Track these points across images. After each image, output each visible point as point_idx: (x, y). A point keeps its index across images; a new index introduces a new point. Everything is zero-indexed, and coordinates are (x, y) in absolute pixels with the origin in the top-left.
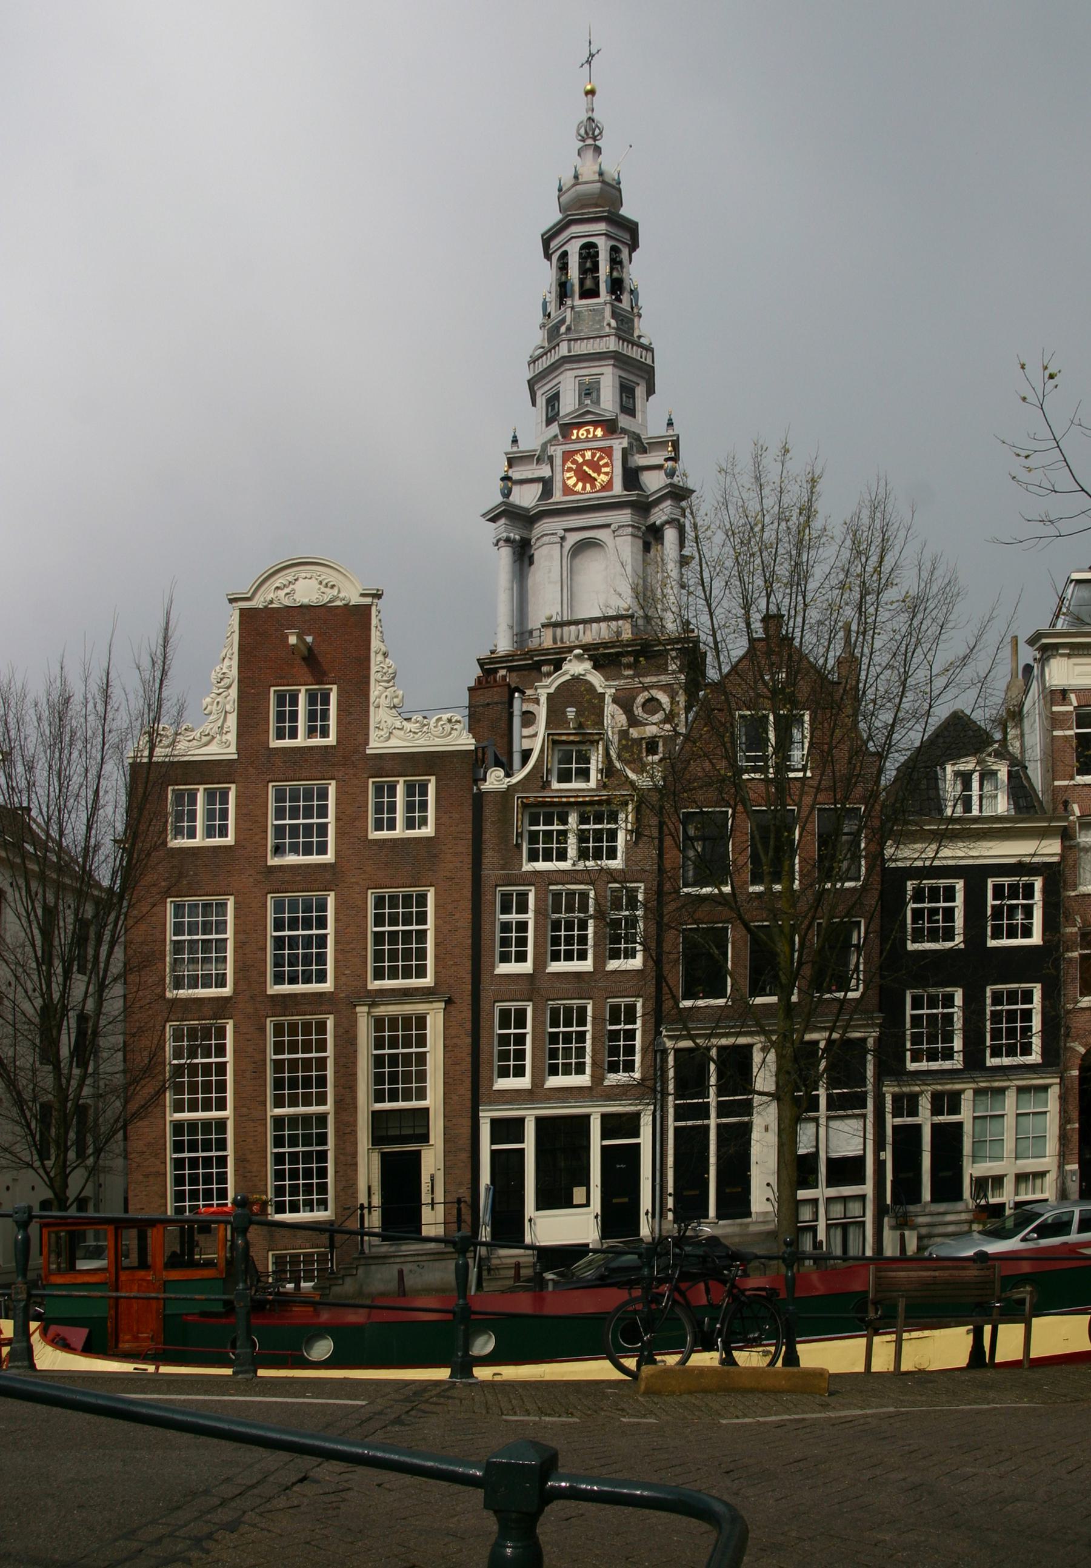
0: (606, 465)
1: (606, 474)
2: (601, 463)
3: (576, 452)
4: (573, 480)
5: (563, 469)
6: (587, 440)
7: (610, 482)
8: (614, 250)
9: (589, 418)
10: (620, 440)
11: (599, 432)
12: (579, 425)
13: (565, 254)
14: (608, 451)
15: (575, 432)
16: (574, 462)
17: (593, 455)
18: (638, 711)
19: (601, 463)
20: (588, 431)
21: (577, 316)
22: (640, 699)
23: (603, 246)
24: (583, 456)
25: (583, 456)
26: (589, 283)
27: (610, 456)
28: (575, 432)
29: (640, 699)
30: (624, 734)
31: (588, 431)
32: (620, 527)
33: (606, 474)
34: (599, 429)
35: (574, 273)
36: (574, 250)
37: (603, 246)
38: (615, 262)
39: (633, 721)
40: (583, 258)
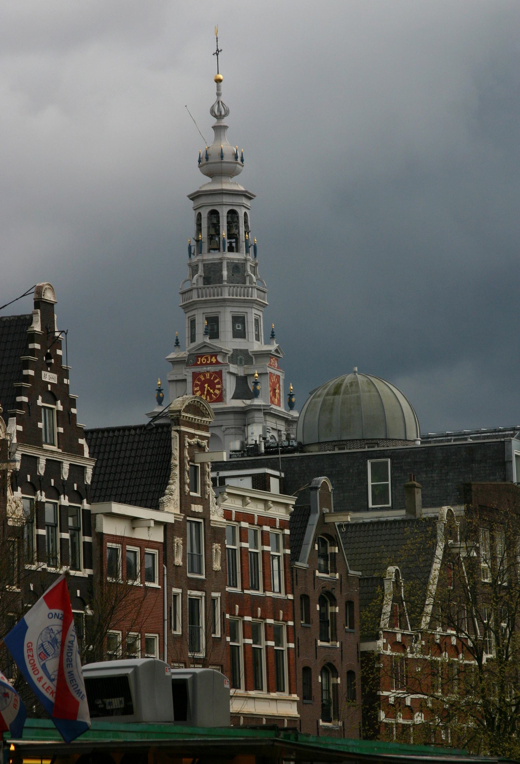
0: (218, 383)
1: (219, 389)
2: (216, 381)
3: (200, 373)
5: (193, 385)
6: (207, 364)
7: (221, 394)
10: (226, 367)
15: (199, 359)
16: (199, 380)
17: (211, 376)
19: (216, 381)
20: (207, 358)
24: (205, 376)
25: (205, 376)
28: (199, 359)
31: (207, 358)
32: (226, 429)
33: (219, 389)
34: (214, 358)
36: (205, 213)
40: (209, 219)
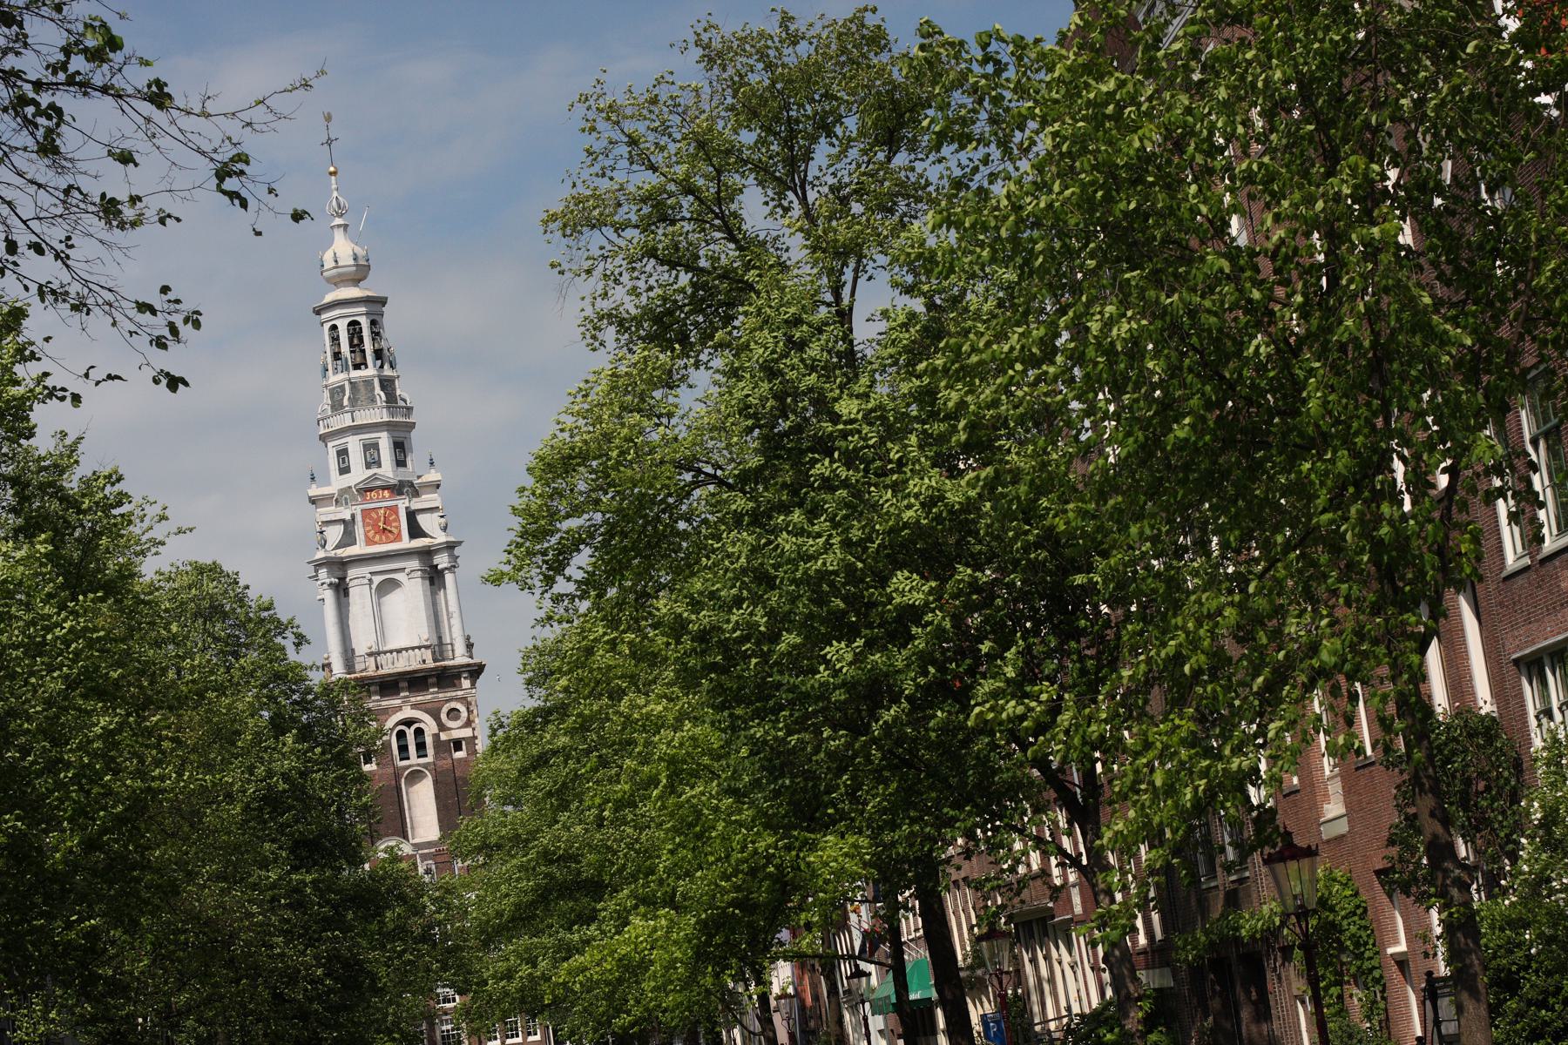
4: (371, 534)
8: (373, 323)
9: (378, 483)
11: (386, 493)
12: (371, 490)
13: (334, 328)
14: (394, 509)
18: (443, 716)
21: (353, 384)
22: (445, 710)
23: (364, 322)
26: (358, 360)
27: (397, 513)
29: (445, 710)
30: (436, 737)
35: (345, 348)
36: (342, 325)
37: (364, 322)
38: (376, 335)
39: (442, 727)
